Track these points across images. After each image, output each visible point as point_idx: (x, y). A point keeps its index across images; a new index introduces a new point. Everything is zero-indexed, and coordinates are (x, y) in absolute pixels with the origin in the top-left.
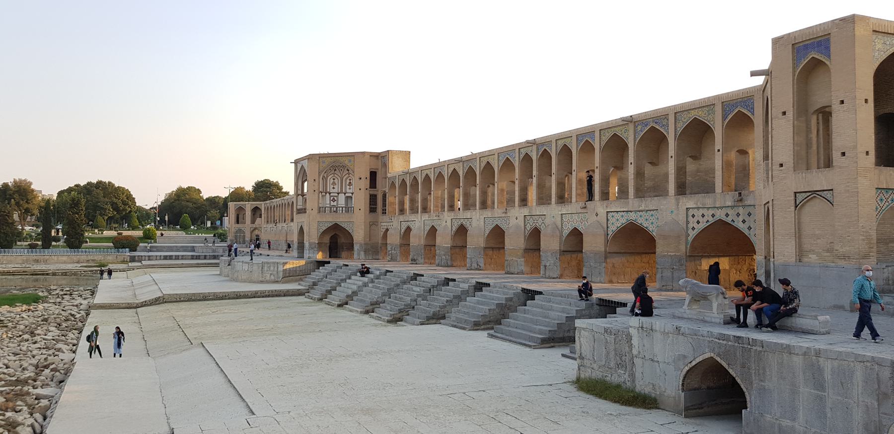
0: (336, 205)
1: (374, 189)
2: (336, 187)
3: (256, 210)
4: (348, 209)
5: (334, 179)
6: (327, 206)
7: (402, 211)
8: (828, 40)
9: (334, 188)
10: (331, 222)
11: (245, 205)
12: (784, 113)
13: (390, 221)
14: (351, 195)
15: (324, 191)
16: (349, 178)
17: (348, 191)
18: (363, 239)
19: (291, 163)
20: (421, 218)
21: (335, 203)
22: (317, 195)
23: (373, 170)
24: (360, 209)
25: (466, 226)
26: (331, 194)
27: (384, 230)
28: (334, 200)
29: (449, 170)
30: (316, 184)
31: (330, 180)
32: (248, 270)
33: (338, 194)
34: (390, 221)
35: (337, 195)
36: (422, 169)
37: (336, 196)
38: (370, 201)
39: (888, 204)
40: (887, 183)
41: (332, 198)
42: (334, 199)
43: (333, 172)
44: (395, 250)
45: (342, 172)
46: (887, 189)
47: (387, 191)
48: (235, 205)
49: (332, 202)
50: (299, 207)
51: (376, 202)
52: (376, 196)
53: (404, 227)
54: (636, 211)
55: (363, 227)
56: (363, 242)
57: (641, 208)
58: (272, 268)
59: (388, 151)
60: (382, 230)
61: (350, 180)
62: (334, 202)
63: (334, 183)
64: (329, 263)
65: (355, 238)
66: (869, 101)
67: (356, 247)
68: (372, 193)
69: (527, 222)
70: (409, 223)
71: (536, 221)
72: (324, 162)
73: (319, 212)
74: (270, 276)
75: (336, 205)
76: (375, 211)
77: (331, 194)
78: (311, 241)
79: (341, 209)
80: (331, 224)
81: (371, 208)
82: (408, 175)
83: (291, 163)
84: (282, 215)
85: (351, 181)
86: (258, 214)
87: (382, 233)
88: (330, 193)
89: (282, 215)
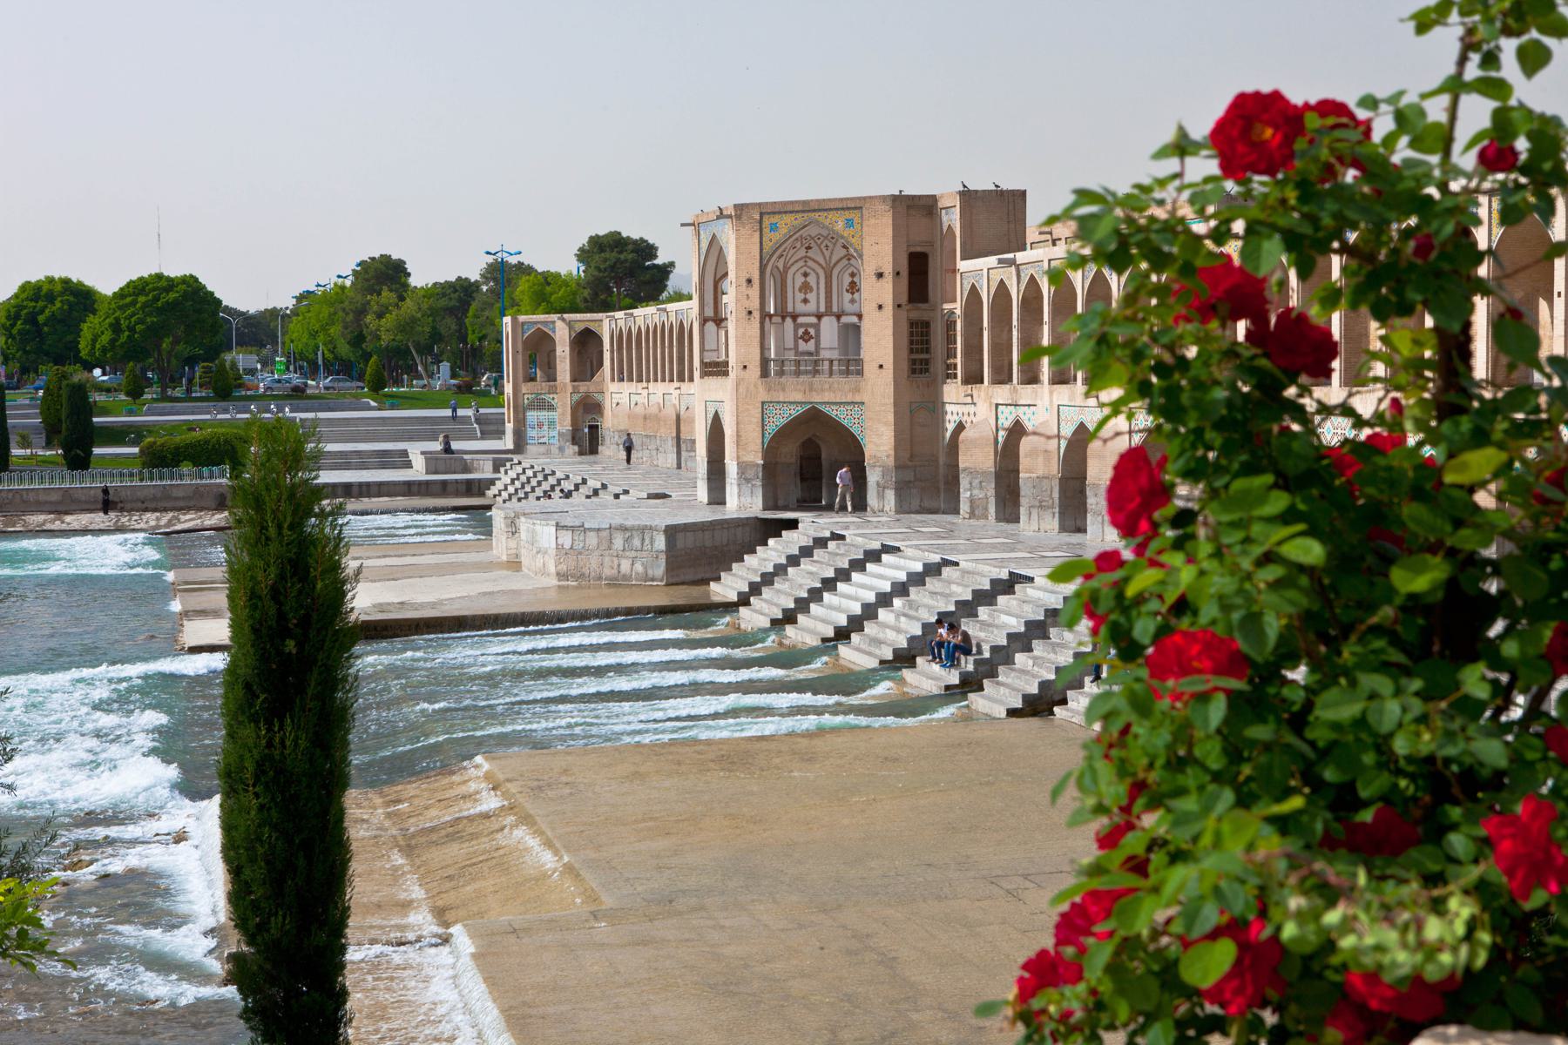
2: (811, 297)
3: (586, 342)
5: (806, 275)
9: (805, 301)
11: (554, 322)
14: (854, 319)
17: (848, 307)
18: (892, 453)
19: (683, 225)
20: (1051, 393)
21: (811, 346)
22: (757, 325)
23: (919, 249)
24: (881, 366)
26: (801, 320)
28: (806, 337)
30: (755, 292)
33: (819, 317)
35: (813, 320)
37: (811, 325)
38: (911, 342)
41: (801, 331)
42: (806, 333)
43: (802, 252)
44: (981, 488)
45: (827, 253)
47: (958, 312)
48: (523, 324)
49: (800, 341)
52: (926, 325)
53: (1007, 418)
55: (891, 417)
56: (891, 462)
58: (637, 542)
61: (853, 275)
62: (806, 341)
63: (806, 288)
64: (793, 524)
65: (869, 451)
67: (873, 477)
68: (915, 315)
72: (774, 228)
73: (765, 373)
76: (927, 370)
77: (801, 320)
78: (745, 459)
80: (801, 410)
81: (914, 362)
83: (683, 225)
88: (794, 317)
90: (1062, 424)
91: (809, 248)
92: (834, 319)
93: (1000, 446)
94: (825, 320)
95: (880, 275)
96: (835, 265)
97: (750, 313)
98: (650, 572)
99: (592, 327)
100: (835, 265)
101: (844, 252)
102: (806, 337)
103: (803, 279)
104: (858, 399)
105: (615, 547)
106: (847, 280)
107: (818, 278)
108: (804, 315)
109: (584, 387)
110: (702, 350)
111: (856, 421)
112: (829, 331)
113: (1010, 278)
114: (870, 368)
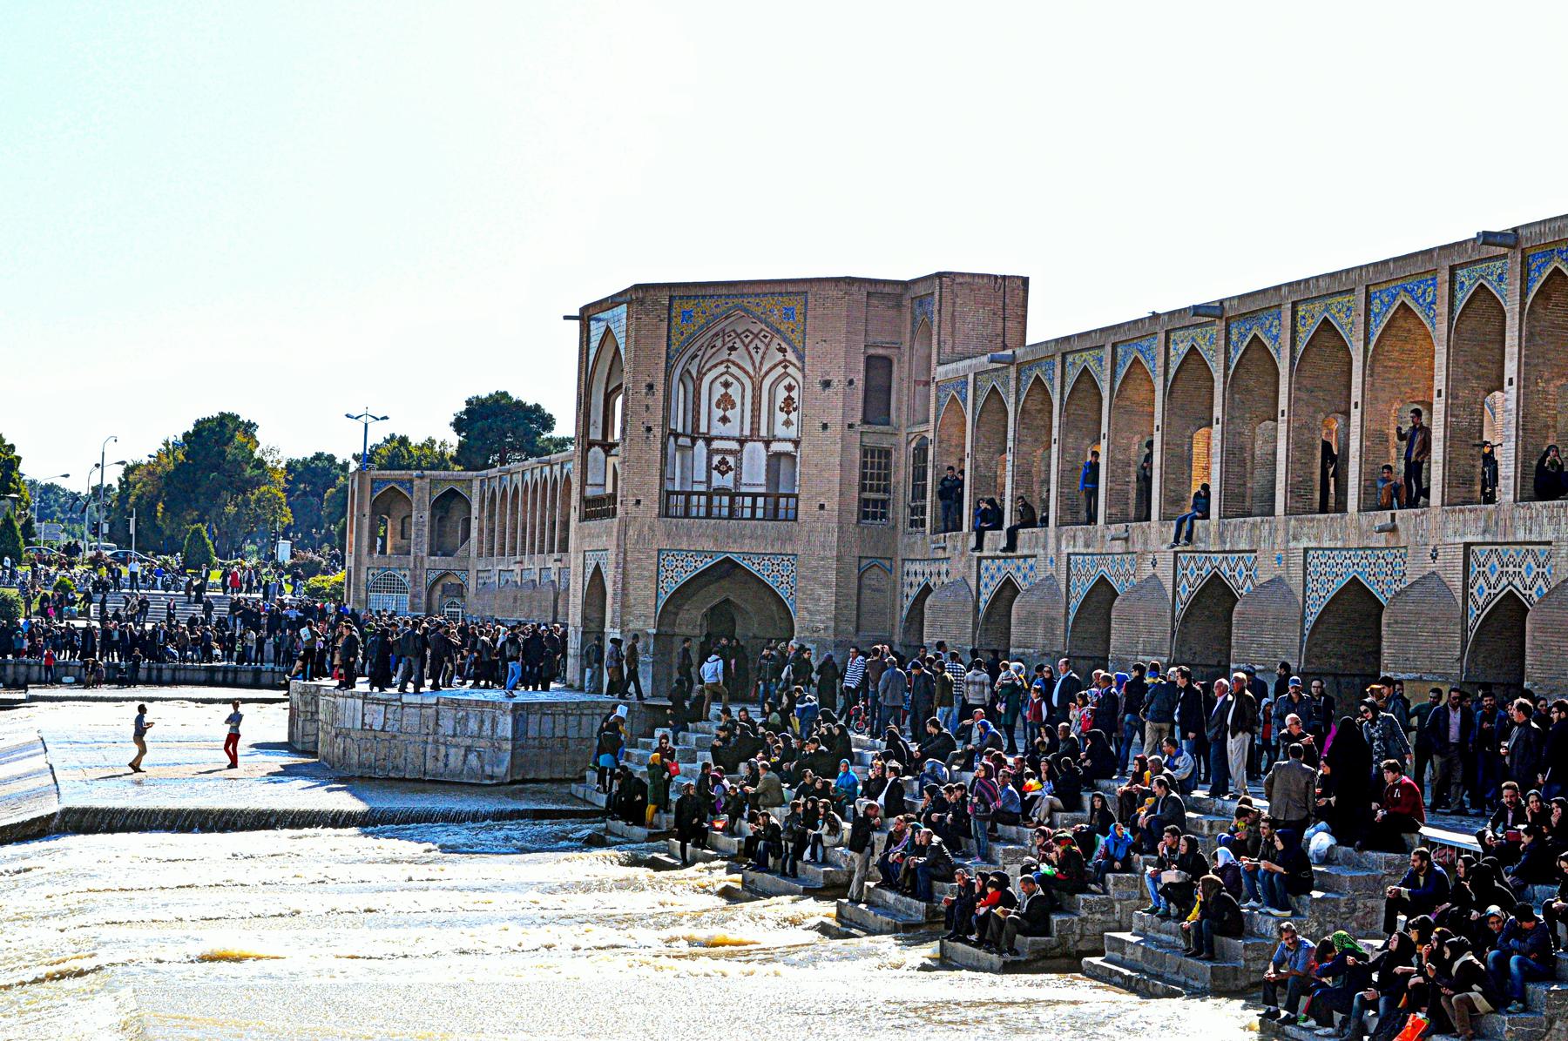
0: (731, 485)
5: (726, 385)
6: (697, 488)
9: (724, 420)
10: (711, 554)
13: (940, 554)
14: (789, 447)
15: (689, 430)
16: (786, 382)
17: (780, 431)
19: (566, 318)
23: (880, 351)
25: (1231, 584)
26: (716, 444)
27: (915, 591)
28: (723, 468)
29: (1172, 352)
32: (383, 730)
33: (742, 442)
34: (940, 554)
35: (734, 446)
36: (1065, 346)
37: (730, 452)
41: (716, 459)
42: (723, 462)
45: (757, 359)
47: (930, 436)
49: (715, 473)
50: (590, 492)
56: (830, 637)
58: (473, 725)
59: (940, 275)
60: (907, 589)
61: (789, 388)
62: (723, 473)
68: (870, 441)
69: (1475, 569)
71: (1511, 569)
72: (687, 316)
73: (665, 513)
74: (466, 756)
75: (731, 485)
77: (716, 444)
79: (748, 501)
80: (710, 562)
81: (865, 503)
82: (1013, 370)
83: (566, 318)
84: (543, 524)
85: (794, 394)
86: (457, 515)
87: (907, 604)
88: (709, 441)
89: (543, 524)
90: (1073, 579)
91: (733, 349)
92: (761, 445)
93: (981, 616)
94: (748, 445)
95: (827, 384)
96: (767, 373)
97: (649, 429)
98: (488, 770)
100: (767, 373)
101: (780, 356)
102: (723, 468)
103: (723, 391)
105: (441, 731)
106: (781, 394)
107: (744, 390)
108: (722, 438)
109: (440, 562)
110: (584, 483)
111: (785, 579)
113: (1006, 384)
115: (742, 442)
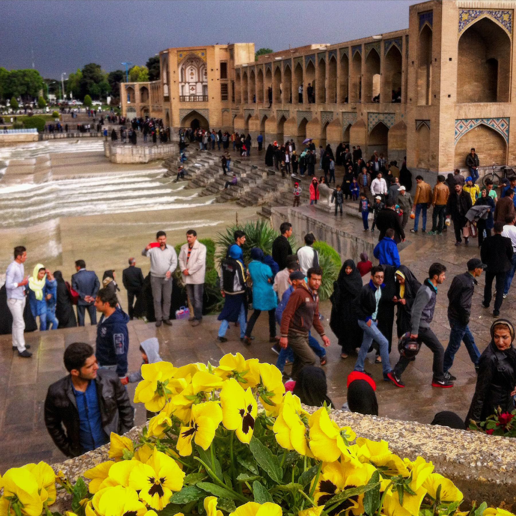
1: (224, 79)
2: (194, 77)
3: (144, 89)
4: (205, 98)
5: (192, 70)
7: (246, 99)
8: (432, 13)
9: (192, 78)
12: (413, 62)
17: (205, 80)
26: (191, 84)
28: (193, 89)
31: (188, 71)
33: (196, 83)
35: (194, 84)
38: (222, 91)
39: (466, 129)
40: (466, 115)
41: (191, 87)
42: (192, 88)
43: (190, 63)
46: (466, 120)
51: (227, 90)
54: (384, 114)
57: (386, 111)
58: (140, 152)
66: (453, 59)
68: (223, 82)
70: (250, 112)
76: (227, 99)
77: (191, 84)
80: (190, 111)
81: (222, 97)
91: (192, 62)
92: (200, 84)
94: (198, 84)
99: (145, 86)
104: (207, 108)
106: (204, 71)
112: (199, 87)
114: (210, 98)
115: (196, 83)
